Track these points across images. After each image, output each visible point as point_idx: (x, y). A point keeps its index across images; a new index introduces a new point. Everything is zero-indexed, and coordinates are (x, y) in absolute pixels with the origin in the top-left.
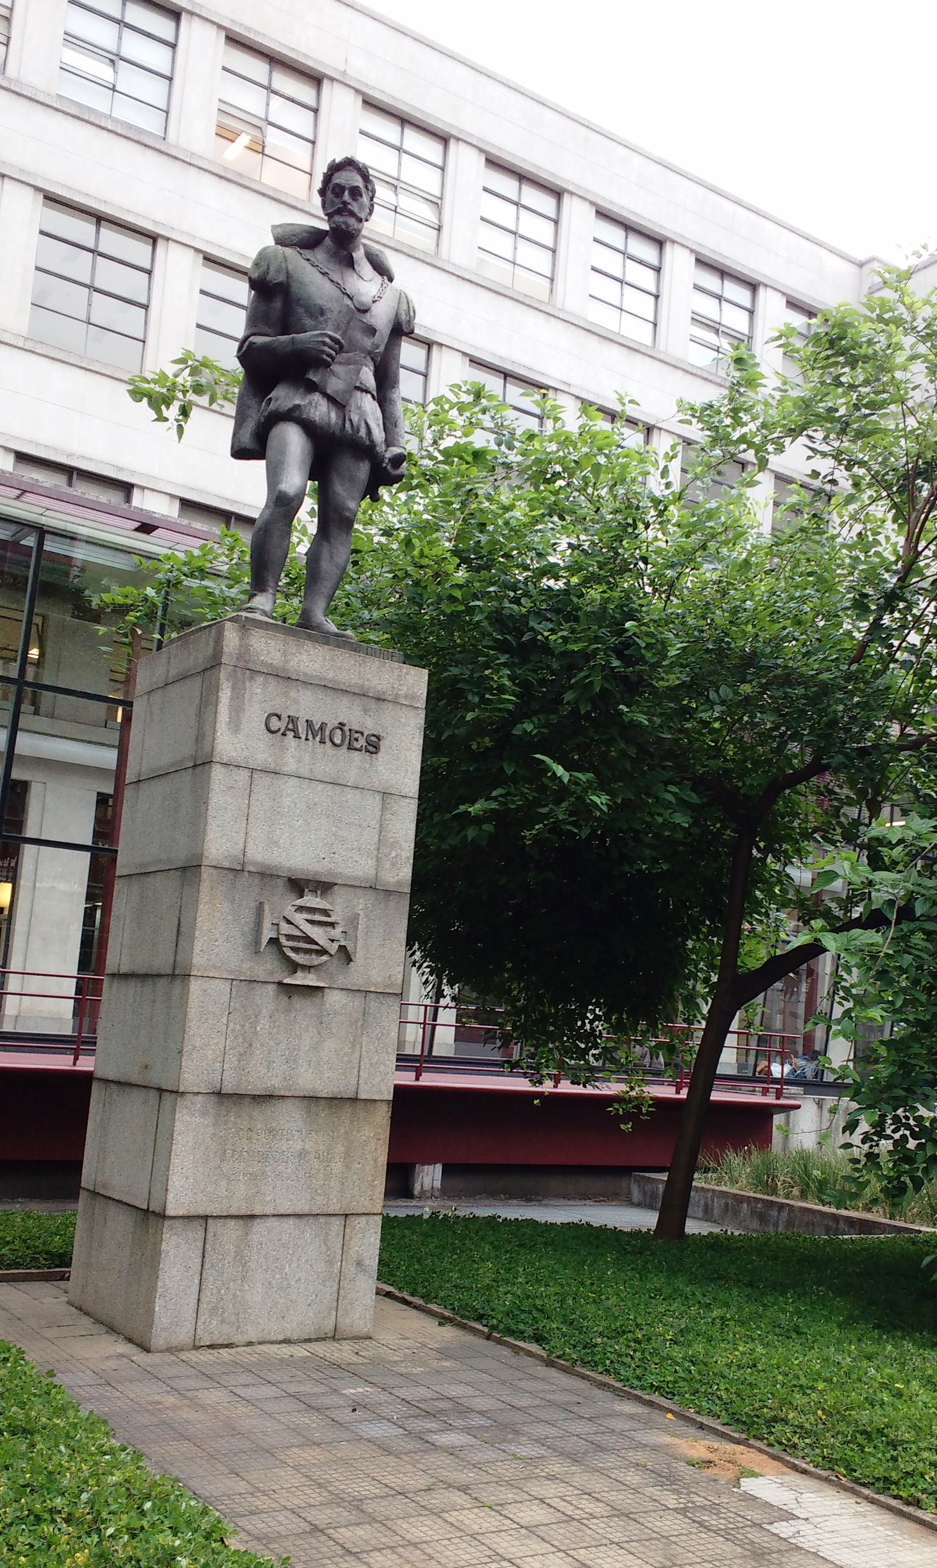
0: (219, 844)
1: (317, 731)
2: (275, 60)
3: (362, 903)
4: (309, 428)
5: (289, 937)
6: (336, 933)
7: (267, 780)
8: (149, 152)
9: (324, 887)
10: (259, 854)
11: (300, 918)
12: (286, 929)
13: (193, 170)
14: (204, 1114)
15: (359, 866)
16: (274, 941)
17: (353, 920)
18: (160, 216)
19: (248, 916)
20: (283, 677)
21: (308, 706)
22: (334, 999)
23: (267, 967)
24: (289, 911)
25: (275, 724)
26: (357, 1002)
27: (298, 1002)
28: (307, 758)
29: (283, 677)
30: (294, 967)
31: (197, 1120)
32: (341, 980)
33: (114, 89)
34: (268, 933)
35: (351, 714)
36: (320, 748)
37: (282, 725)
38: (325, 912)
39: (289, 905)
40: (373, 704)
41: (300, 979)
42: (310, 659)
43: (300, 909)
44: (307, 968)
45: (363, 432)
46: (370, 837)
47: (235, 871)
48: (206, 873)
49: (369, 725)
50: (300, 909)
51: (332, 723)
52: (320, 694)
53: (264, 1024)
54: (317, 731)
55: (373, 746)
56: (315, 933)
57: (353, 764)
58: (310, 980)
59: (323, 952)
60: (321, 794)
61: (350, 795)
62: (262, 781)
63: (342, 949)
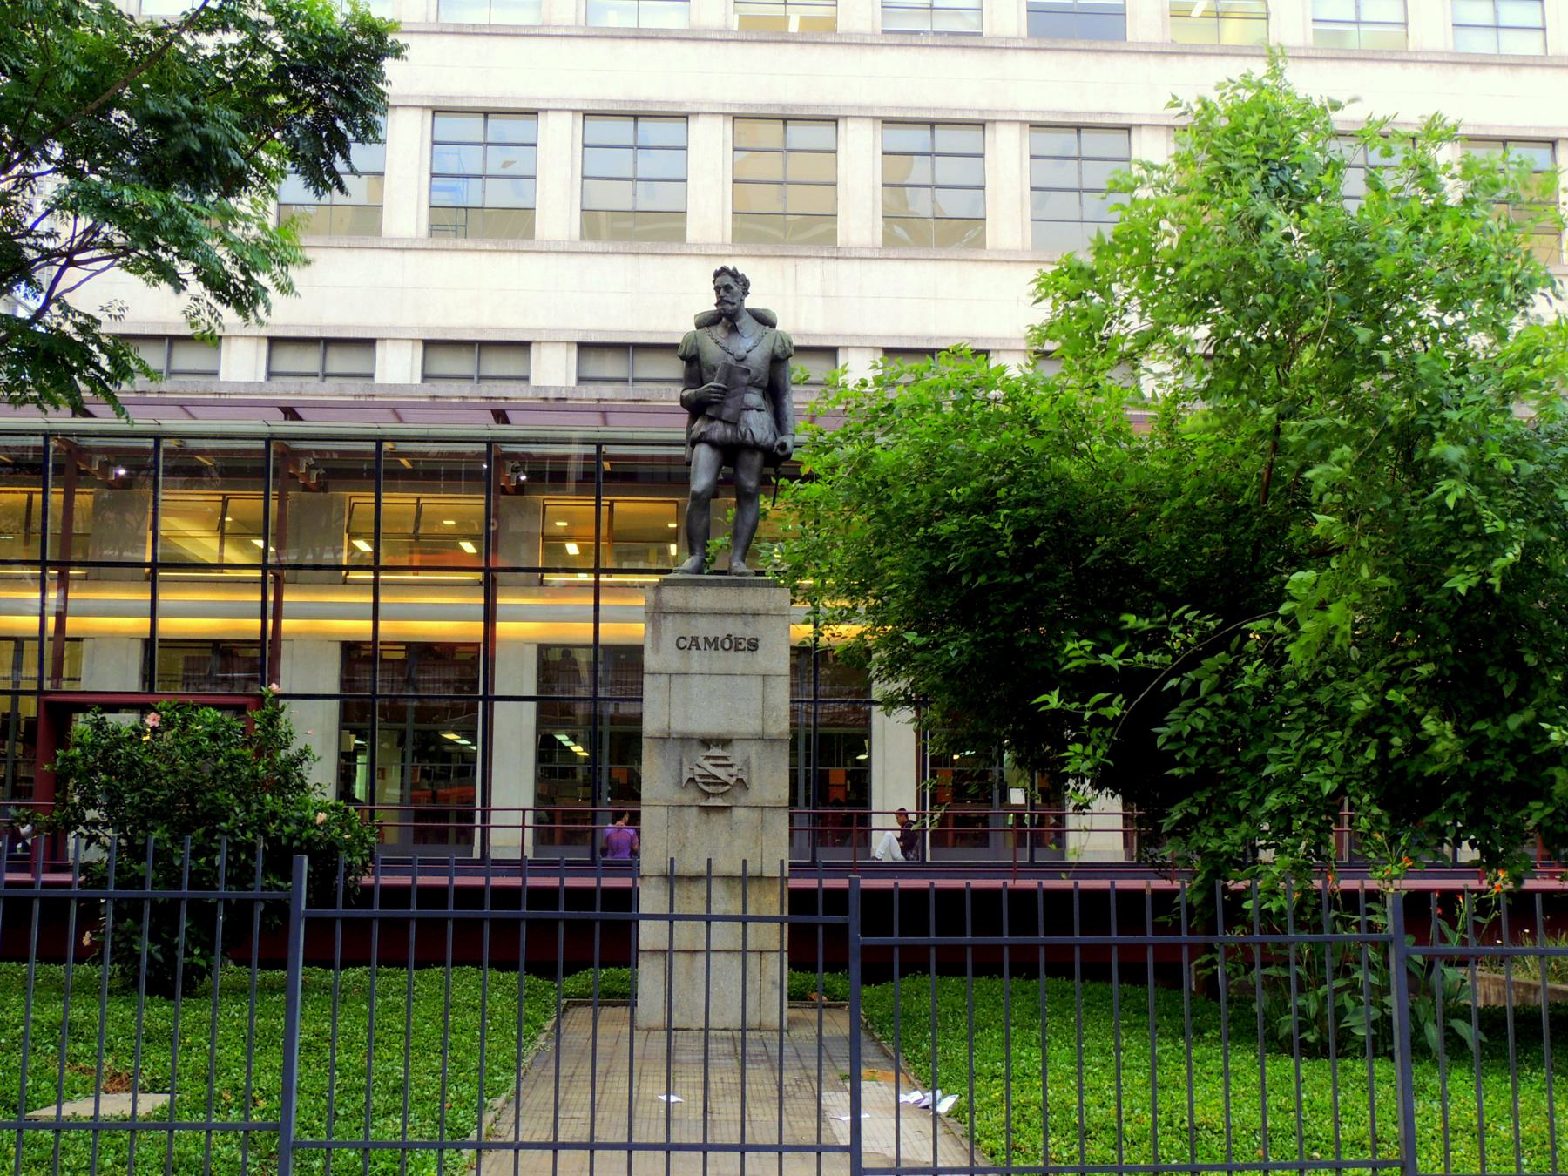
0: (651, 724)
1: (713, 643)
3: (754, 750)
4: (713, 444)
5: (701, 776)
6: (734, 771)
7: (681, 679)
8: (968, 52)
9: (725, 742)
10: (678, 726)
11: (707, 764)
12: (698, 771)
13: (1010, 53)
14: (658, 889)
15: (751, 725)
16: (692, 780)
17: (747, 762)
18: (983, 103)
19: (675, 764)
20: (686, 613)
21: (705, 628)
22: (739, 813)
23: (690, 796)
24: (700, 760)
25: (683, 643)
26: (756, 815)
27: (714, 817)
28: (706, 662)
29: (686, 613)
30: (708, 795)
31: (653, 891)
32: (743, 800)
33: (931, 8)
34: (686, 776)
35: (736, 628)
36: (715, 654)
37: (687, 643)
38: (725, 758)
39: (700, 755)
40: (750, 619)
41: (712, 802)
42: (704, 598)
43: (708, 758)
44: (714, 795)
45: (748, 438)
47: (664, 739)
48: (645, 742)
49: (749, 633)
50: (708, 758)
51: (721, 636)
52: (711, 618)
53: (691, 832)
54: (713, 643)
55: (753, 645)
56: (719, 772)
57: (739, 660)
58: (719, 802)
59: (726, 784)
61: (739, 680)
62: (676, 680)
63: (740, 780)
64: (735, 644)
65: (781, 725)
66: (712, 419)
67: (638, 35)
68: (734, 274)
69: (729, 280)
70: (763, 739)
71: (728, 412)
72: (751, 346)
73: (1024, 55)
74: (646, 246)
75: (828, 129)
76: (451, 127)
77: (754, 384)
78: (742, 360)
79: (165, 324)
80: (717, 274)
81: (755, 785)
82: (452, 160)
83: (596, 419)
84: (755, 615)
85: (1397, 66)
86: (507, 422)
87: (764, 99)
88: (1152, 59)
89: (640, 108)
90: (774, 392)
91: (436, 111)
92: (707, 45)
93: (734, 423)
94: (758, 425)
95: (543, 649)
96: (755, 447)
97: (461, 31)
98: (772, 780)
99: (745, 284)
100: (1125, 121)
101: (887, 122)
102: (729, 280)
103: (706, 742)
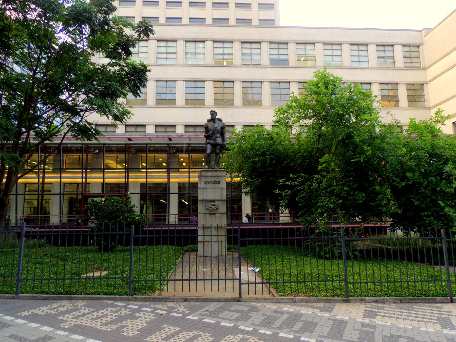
0: (200, 198)
1: (211, 182)
2: (278, 43)
3: (219, 203)
4: (211, 144)
9: (214, 201)
10: (205, 198)
15: (219, 198)
20: (206, 177)
21: (210, 179)
22: (217, 215)
26: (220, 215)
27: (212, 216)
32: (218, 212)
35: (215, 179)
41: (212, 213)
42: (209, 174)
46: (220, 194)
47: (202, 201)
49: (218, 180)
54: (211, 182)
55: (219, 183)
57: (216, 186)
58: (213, 213)
60: (212, 190)
64: (216, 182)
65: (225, 198)
66: (210, 139)
67: (195, 66)
68: (214, 112)
69: (213, 113)
70: (221, 200)
71: (213, 138)
72: (218, 125)
73: (269, 68)
74: (198, 106)
75: (232, 83)
76: (159, 84)
77: (218, 133)
78: (216, 128)
79: (105, 123)
80: (211, 112)
81: (220, 209)
82: (160, 90)
83: (188, 139)
84: (219, 177)
85: (340, 70)
86: (171, 140)
87: (219, 78)
88: (294, 69)
89: (196, 80)
90: (222, 134)
91: (157, 81)
92: (208, 67)
93: (215, 140)
94: (219, 140)
95: (179, 184)
96: (219, 145)
97: (161, 65)
98: (223, 208)
99: (216, 113)
100: (289, 81)
101: (243, 82)
102: (213, 113)
103: (210, 201)
